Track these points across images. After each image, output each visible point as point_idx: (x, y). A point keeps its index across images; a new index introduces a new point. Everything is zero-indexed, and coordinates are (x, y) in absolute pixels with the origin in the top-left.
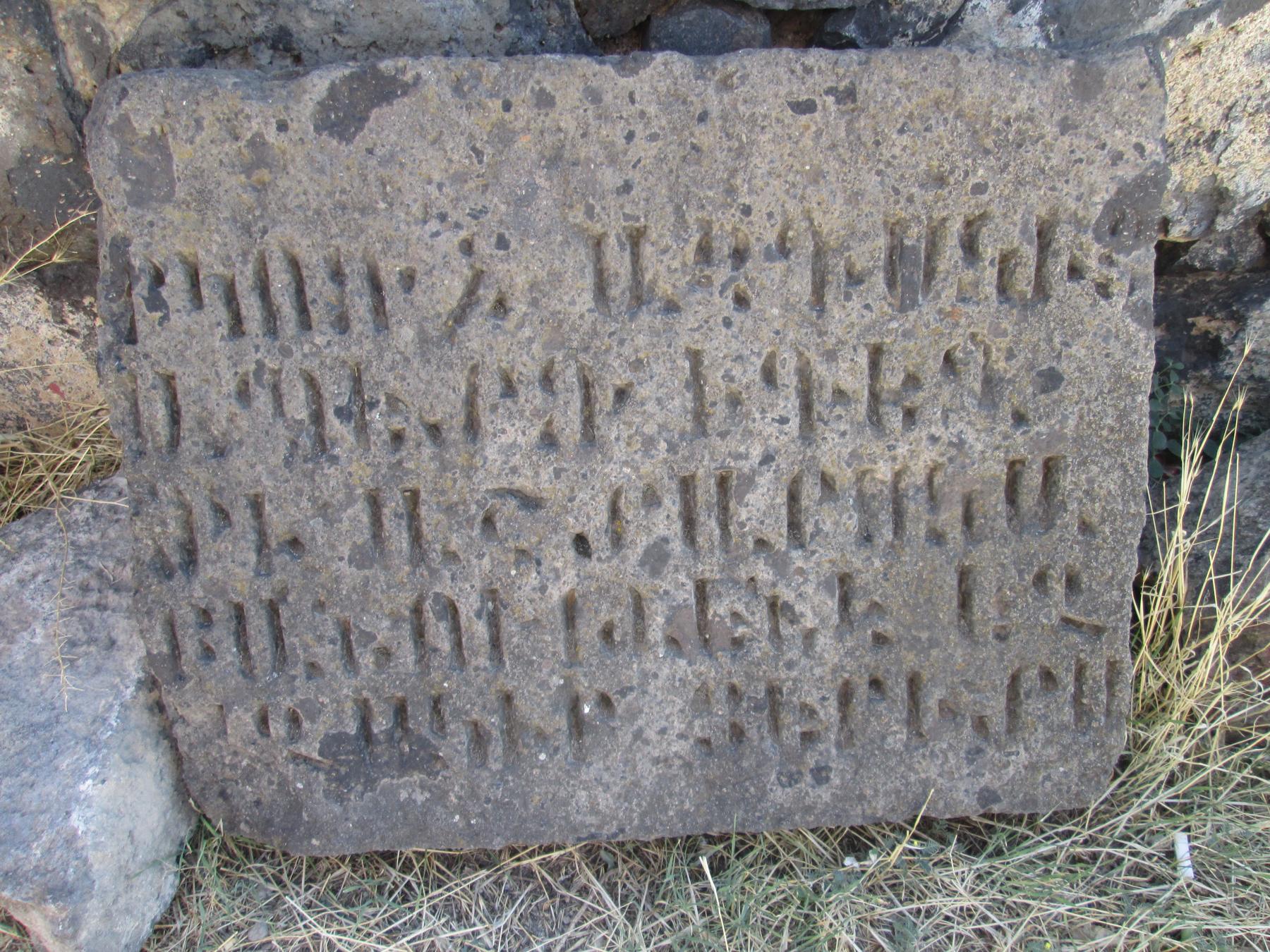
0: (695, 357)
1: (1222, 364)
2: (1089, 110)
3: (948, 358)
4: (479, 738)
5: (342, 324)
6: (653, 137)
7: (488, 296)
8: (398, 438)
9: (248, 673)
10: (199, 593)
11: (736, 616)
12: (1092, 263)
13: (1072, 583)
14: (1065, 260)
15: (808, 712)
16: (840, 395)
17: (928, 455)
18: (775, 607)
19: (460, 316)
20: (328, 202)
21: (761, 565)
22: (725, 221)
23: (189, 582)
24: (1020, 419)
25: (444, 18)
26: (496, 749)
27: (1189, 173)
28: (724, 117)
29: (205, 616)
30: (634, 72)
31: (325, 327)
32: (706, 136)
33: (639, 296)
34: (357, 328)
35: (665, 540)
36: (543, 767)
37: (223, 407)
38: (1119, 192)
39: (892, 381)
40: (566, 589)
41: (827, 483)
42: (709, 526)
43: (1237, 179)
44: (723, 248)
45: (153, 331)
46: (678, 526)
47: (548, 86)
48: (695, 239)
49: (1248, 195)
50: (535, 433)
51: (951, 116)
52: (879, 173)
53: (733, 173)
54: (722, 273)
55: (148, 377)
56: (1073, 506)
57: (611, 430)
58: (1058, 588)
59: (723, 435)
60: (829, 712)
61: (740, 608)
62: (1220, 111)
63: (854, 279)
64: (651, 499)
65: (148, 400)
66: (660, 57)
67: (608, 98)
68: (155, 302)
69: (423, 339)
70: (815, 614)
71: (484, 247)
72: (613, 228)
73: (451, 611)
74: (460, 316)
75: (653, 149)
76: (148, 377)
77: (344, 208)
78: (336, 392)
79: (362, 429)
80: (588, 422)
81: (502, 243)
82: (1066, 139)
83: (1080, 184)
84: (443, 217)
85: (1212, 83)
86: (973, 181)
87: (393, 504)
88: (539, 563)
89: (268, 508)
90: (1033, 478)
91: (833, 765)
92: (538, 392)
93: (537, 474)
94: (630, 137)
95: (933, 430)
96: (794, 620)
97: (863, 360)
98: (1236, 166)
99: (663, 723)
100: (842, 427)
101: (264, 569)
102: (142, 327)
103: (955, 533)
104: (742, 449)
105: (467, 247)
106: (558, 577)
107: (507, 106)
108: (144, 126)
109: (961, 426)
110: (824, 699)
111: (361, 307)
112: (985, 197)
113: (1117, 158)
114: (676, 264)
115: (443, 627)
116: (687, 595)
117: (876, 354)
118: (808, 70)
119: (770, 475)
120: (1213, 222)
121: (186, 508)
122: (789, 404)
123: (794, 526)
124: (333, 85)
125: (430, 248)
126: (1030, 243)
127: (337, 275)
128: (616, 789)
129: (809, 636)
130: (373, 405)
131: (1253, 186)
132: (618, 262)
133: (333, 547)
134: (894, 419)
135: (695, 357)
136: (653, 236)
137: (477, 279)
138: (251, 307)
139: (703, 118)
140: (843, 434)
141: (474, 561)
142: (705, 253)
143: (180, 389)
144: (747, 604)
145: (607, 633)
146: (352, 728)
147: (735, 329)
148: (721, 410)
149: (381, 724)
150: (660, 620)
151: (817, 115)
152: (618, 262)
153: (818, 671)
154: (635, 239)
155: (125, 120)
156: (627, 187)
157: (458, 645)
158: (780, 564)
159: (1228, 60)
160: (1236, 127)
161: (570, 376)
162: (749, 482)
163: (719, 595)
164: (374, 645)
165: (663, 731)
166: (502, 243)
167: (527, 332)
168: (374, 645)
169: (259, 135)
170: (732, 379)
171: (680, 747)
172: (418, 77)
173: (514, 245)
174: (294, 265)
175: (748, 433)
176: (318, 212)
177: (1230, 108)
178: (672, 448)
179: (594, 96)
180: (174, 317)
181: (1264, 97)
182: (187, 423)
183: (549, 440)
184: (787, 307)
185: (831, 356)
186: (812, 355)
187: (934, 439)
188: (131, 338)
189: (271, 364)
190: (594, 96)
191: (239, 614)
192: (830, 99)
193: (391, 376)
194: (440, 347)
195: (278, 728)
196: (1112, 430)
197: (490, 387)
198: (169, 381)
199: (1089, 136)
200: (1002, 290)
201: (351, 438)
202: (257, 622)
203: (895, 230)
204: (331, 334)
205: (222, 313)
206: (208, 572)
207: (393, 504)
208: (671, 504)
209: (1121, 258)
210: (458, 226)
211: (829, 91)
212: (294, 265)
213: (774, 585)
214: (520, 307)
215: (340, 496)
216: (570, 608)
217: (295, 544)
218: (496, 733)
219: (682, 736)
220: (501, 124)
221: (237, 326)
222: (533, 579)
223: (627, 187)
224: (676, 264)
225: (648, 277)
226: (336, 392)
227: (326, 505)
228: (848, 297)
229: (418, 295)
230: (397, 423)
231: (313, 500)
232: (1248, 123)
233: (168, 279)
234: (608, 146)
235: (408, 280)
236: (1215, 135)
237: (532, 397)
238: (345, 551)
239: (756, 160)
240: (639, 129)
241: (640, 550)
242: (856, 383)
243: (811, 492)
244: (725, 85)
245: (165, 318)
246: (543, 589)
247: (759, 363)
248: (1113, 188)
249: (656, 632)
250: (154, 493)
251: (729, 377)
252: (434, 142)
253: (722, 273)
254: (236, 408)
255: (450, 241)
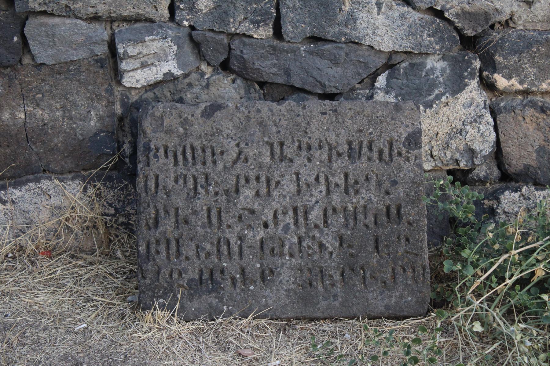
0: (297, 174)
1: (497, 217)
2: (399, 114)
3: (367, 177)
4: (234, 281)
5: (204, 163)
6: (286, 120)
7: (242, 157)
8: (217, 193)
9: (168, 258)
10: (157, 235)
11: (309, 247)
12: (403, 152)
13: (407, 240)
14: (396, 151)
15: (331, 276)
16: (337, 185)
17: (362, 203)
18: (321, 246)
19: (235, 162)
20: (203, 133)
21: (316, 232)
22: (305, 140)
23: (155, 231)
24: (387, 193)
25: (226, 95)
26: (239, 284)
27: (458, 143)
28: (304, 115)
29: (158, 242)
30: (281, 105)
31: (200, 164)
32: (299, 119)
33: (282, 158)
34: (208, 165)
35: (289, 224)
36: (252, 291)
37: (171, 182)
38: (408, 135)
39: (351, 181)
40: (261, 237)
41: (334, 210)
42: (301, 220)
43: (474, 145)
44: (304, 146)
45: (154, 163)
46: (292, 220)
47: (260, 108)
48: (297, 144)
49: (481, 151)
50: (254, 193)
51: (362, 116)
52: (344, 129)
53: (306, 128)
54: (304, 153)
55: (152, 175)
56: (404, 218)
57: (275, 193)
58: (403, 241)
59: (304, 195)
60: (337, 277)
61: (310, 244)
62: (461, 123)
63: (339, 155)
64: (285, 213)
65: (151, 182)
66: (287, 102)
67: (274, 111)
68: (156, 156)
69: (225, 167)
70: (332, 247)
71: (242, 145)
72: (275, 141)
73: (228, 243)
74: (235, 162)
75: (286, 123)
76: (152, 175)
77: (206, 134)
78: (201, 180)
79: (207, 191)
80: (269, 192)
81: (247, 145)
82: (393, 122)
83: (398, 132)
84: (232, 138)
85: (455, 114)
86: (369, 132)
87: (214, 212)
88: (253, 229)
89: (180, 211)
90: (394, 211)
91: (338, 294)
92: (255, 182)
93: (254, 204)
94: (280, 120)
95: (362, 195)
96: (326, 248)
97: (342, 176)
98: (472, 140)
99: (288, 278)
100: (337, 194)
101: (177, 227)
102: (151, 163)
103: (372, 225)
104: (310, 199)
105: (238, 145)
106: (258, 234)
107: (249, 112)
108: (158, 114)
109: (370, 194)
110: (335, 273)
111: (209, 159)
112: (373, 136)
113: (407, 126)
114: (292, 151)
115: (225, 247)
116: (295, 240)
117: (346, 176)
118: (325, 105)
119: (318, 206)
120: (473, 161)
121: (157, 211)
122: (323, 188)
123: (326, 222)
124: (206, 107)
125: (228, 145)
126: (386, 147)
127: (204, 151)
128: (273, 299)
129: (331, 253)
130: (210, 185)
131: (482, 148)
132: (277, 150)
133: (196, 222)
134: (352, 192)
135: (297, 174)
136: (286, 143)
137: (240, 153)
138: (180, 158)
139: (299, 115)
140: (338, 196)
141: (235, 228)
142: (300, 147)
143: (159, 178)
144: (312, 243)
145: (272, 250)
146: (197, 277)
147: (307, 167)
148: (304, 188)
149: (206, 276)
150: (287, 247)
151: (328, 115)
152: (277, 150)
153: (333, 264)
154: (282, 144)
155: (153, 113)
156: (279, 132)
157: (229, 253)
158: (321, 232)
159: (458, 107)
160: (468, 128)
161: (263, 178)
162: (312, 208)
163: (304, 241)
164: (205, 252)
165: (288, 281)
166: (247, 145)
167: (253, 167)
168: (205, 252)
169: (187, 117)
170: (307, 180)
171: (292, 286)
172: (228, 105)
173: (250, 145)
174: (193, 149)
175: (312, 195)
176: (200, 136)
177: (463, 122)
178: (291, 198)
179: (271, 111)
180: (160, 160)
181: (472, 118)
182: (161, 187)
183: (258, 194)
184: (321, 162)
185: (333, 175)
186: (328, 174)
187: (363, 198)
188: (148, 165)
189: (184, 173)
190: (271, 111)
191: (168, 242)
192: (331, 112)
193: (216, 177)
194: (229, 170)
195: (175, 276)
196: (413, 196)
197: (242, 181)
198: (157, 177)
199: (399, 121)
200: (381, 159)
201: (204, 193)
202: (173, 244)
203: (350, 143)
204: (201, 166)
205: (173, 160)
206: (161, 229)
207: (214, 212)
208: (291, 213)
209: (411, 152)
210: (235, 140)
211: (330, 110)
212: (193, 149)
213: (320, 238)
214: (250, 161)
215: (200, 208)
216: (262, 242)
217: (186, 222)
218: (238, 280)
219: (293, 283)
220: (248, 116)
221: (176, 163)
222: (251, 234)
223: (279, 132)
224: (292, 151)
225: (284, 154)
226: (201, 180)
227: (196, 211)
228: (337, 160)
229: (225, 157)
230: (217, 189)
231: (192, 210)
232: (471, 126)
233: (160, 151)
234: (274, 121)
235: (222, 153)
236: (461, 130)
237: (253, 183)
238: (200, 223)
239: (312, 126)
240: (282, 118)
241: (282, 226)
242: (341, 182)
243: (329, 212)
244: (304, 108)
245: (158, 160)
246: (254, 236)
247: (314, 177)
248: (407, 134)
249: (286, 250)
250: (149, 206)
251: (306, 180)
252: (230, 120)
253: (304, 153)
254: (173, 183)
255: (233, 143)
